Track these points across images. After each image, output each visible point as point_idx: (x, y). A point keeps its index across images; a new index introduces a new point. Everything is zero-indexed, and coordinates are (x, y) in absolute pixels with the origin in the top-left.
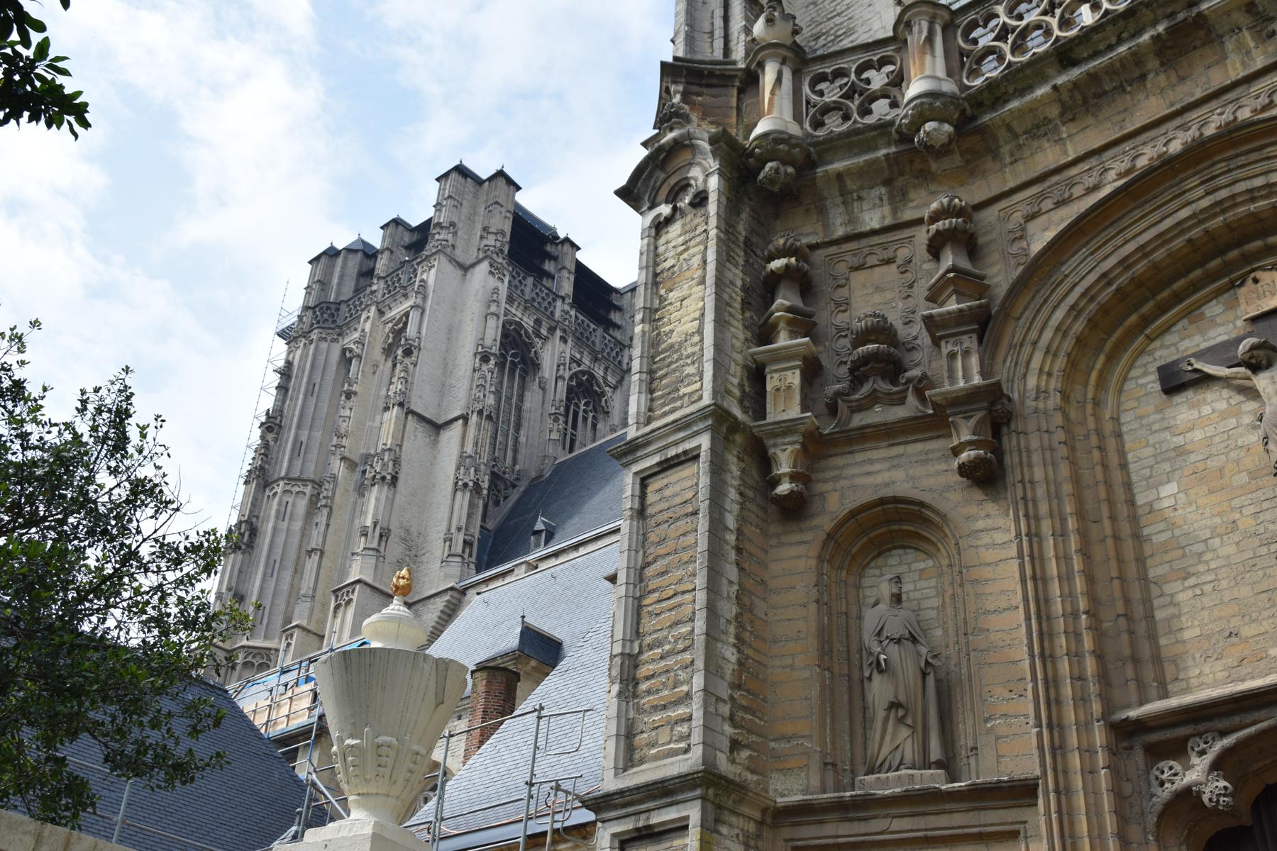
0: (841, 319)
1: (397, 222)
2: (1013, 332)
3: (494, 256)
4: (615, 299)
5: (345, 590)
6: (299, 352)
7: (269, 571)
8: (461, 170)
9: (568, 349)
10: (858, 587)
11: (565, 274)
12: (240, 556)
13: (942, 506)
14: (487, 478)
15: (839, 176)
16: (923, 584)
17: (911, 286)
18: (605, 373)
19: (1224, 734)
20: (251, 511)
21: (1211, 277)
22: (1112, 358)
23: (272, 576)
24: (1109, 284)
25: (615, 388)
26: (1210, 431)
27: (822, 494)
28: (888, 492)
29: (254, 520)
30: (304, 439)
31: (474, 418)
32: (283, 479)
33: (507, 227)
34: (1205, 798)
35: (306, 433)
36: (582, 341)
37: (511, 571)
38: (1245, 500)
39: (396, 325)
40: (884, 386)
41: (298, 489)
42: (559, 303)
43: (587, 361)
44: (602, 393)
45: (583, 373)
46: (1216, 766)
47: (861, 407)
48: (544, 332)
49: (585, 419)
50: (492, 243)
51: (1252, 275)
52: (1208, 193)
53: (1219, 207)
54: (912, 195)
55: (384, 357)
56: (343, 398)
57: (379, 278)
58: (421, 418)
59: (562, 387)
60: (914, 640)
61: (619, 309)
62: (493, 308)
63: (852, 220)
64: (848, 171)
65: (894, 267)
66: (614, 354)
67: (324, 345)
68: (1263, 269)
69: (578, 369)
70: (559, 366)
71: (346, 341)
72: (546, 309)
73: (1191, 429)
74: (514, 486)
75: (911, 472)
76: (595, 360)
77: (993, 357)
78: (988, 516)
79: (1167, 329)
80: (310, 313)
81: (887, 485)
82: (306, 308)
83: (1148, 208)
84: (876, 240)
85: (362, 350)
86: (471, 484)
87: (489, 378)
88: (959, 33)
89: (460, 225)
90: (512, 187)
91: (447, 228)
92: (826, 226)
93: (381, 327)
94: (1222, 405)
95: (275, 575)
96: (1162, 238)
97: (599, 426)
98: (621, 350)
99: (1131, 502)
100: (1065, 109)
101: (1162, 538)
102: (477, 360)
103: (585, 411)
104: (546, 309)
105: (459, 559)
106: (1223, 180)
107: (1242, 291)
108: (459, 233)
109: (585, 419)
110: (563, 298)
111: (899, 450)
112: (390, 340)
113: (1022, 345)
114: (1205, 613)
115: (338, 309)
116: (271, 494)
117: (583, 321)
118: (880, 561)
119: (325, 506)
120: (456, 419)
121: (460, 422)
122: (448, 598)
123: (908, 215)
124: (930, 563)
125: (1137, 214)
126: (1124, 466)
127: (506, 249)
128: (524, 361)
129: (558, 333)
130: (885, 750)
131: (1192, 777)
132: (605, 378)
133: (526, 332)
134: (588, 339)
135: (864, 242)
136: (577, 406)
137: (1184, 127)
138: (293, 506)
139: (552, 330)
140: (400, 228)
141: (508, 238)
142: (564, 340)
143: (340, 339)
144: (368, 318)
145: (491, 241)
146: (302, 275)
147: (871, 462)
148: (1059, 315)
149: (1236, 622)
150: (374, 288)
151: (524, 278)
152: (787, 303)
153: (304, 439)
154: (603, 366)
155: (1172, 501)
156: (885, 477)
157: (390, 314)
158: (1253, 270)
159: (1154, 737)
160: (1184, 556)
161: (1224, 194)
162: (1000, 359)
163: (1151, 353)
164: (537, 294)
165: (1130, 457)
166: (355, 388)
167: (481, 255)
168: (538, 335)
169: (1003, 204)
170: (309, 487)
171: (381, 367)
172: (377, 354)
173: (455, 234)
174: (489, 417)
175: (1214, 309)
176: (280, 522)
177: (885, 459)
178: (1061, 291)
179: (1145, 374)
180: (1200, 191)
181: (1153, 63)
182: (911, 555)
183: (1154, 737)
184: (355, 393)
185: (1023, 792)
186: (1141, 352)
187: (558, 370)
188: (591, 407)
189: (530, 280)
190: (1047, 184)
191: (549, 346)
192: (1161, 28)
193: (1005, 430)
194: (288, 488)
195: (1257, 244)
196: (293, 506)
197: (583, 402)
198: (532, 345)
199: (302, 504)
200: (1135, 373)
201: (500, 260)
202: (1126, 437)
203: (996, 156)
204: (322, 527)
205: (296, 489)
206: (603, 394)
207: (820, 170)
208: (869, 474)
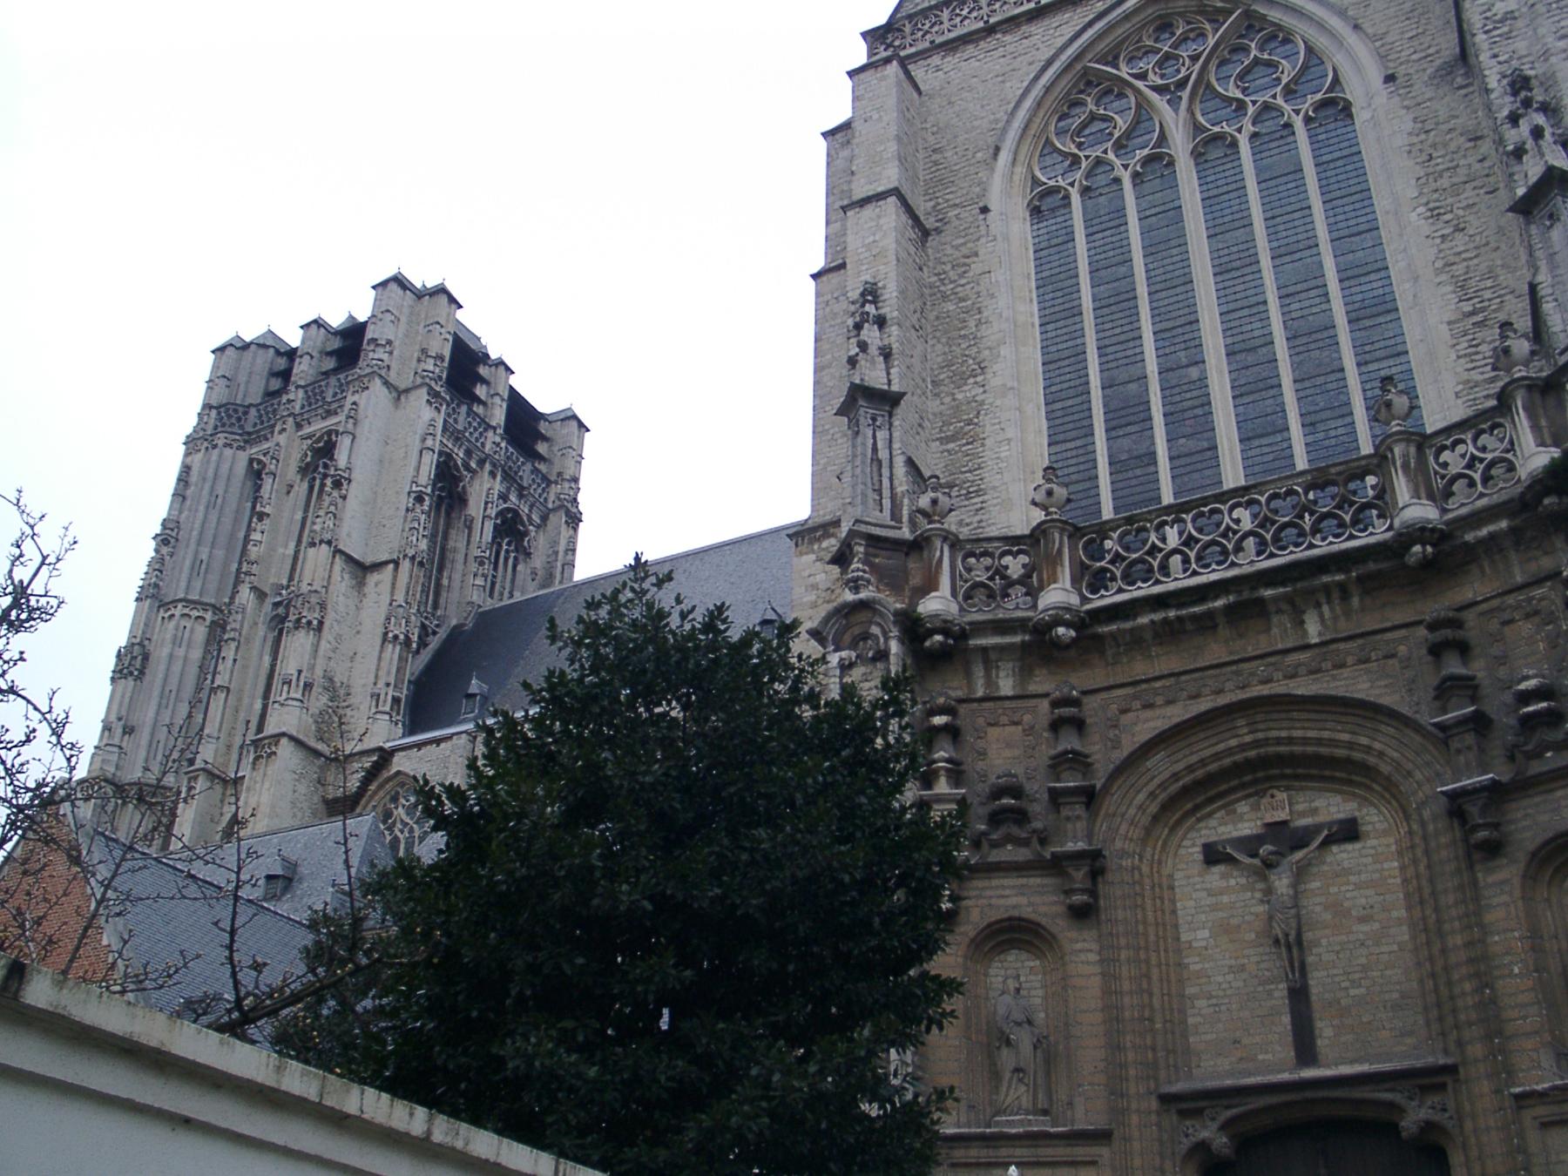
0: (980, 765)
1: (318, 323)
2: (1109, 804)
3: (433, 384)
4: (543, 427)
7: (164, 701)
8: (399, 281)
10: (986, 975)
11: (497, 400)
12: (131, 682)
13: (1054, 929)
14: (416, 631)
15: (984, 650)
16: (1032, 978)
17: (1034, 749)
19: (1228, 1107)
20: (144, 633)
21: (1243, 786)
22: (1173, 829)
23: (167, 707)
24: (1177, 780)
25: (538, 527)
26: (1233, 898)
27: (967, 908)
28: (1016, 913)
29: (146, 642)
30: (204, 557)
31: (406, 565)
33: (447, 353)
34: (1213, 1147)
35: (207, 550)
36: (510, 477)
37: (450, 737)
38: (1251, 951)
39: (315, 442)
40: (1015, 831)
41: (197, 614)
43: (513, 498)
45: (508, 510)
46: (1223, 1128)
47: (995, 845)
48: (473, 465)
49: (506, 559)
50: (431, 368)
51: (1270, 792)
52: (1251, 732)
53: (1256, 744)
54: (1037, 672)
55: (299, 477)
56: (255, 520)
57: (298, 387)
58: (350, 559)
59: (489, 527)
60: (1029, 1022)
61: (545, 439)
62: (429, 443)
63: (990, 682)
64: (996, 648)
65: (1020, 728)
66: (539, 491)
67: (228, 452)
68: (1278, 788)
70: (486, 503)
71: (253, 451)
72: (477, 440)
73: (1221, 894)
74: (435, 633)
75: (1032, 899)
76: (521, 496)
77: (1095, 821)
78: (1084, 940)
79: (1210, 815)
80: (214, 413)
81: (1014, 907)
82: (207, 406)
83: (1210, 732)
84: (1007, 704)
86: (402, 637)
87: (422, 522)
88: (1080, 546)
89: (396, 343)
90: (454, 306)
91: (384, 346)
92: (970, 685)
93: (298, 441)
94: (1243, 881)
95: (171, 707)
96: (1217, 757)
97: (519, 568)
98: (548, 486)
99: (1178, 939)
100: (1156, 635)
101: (1198, 967)
102: (411, 500)
103: (507, 551)
104: (477, 440)
105: (387, 717)
106: (1261, 726)
107: (1265, 801)
108: (395, 353)
109: (506, 559)
111: (1024, 881)
112: (309, 459)
113: (1114, 815)
114: (1220, 1025)
115: (246, 413)
116: (166, 615)
118: (1002, 956)
119: (233, 639)
120: (386, 563)
121: (391, 566)
122: (375, 758)
123: (1033, 688)
124: (1038, 963)
125: (1202, 735)
126: (1174, 912)
127: (444, 376)
128: (450, 496)
130: (1009, 1100)
131: (1204, 1134)
133: (456, 464)
134: (516, 473)
135: (999, 703)
136: (500, 545)
137: (1238, 673)
138: (192, 631)
139: (481, 463)
140: (322, 330)
141: (446, 364)
142: (493, 474)
145: (430, 365)
146: (203, 366)
147: (1003, 887)
148: (1141, 797)
149: (1238, 1034)
150: (292, 396)
151: (458, 405)
152: (946, 755)
153: (204, 557)
155: (1204, 944)
156: (1014, 901)
157: (307, 430)
158: (1271, 787)
159: (1184, 1106)
160: (1210, 983)
161: (1260, 735)
162: (1098, 824)
163: (1198, 830)
164: (470, 423)
165: (1178, 904)
166: (267, 510)
167: (419, 380)
169: (1104, 695)
170: (210, 613)
171: (296, 488)
172: (291, 473)
173: (391, 353)
174: (421, 564)
175: (1243, 808)
176: (177, 649)
177: (1013, 887)
178: (1144, 779)
179: (1194, 845)
180: (1245, 730)
181: (1221, 620)
182: (1024, 955)
183: (1184, 1106)
184: (268, 515)
185: (1101, 1136)
186: (1191, 828)
187: (485, 509)
188: (512, 548)
189: (464, 409)
190: (1138, 689)
191: (476, 483)
192: (1231, 598)
193: (1100, 879)
194: (186, 611)
195: (1276, 772)
196: (192, 631)
197: (506, 540)
198: (459, 479)
199: (201, 632)
200: (1185, 843)
201: (438, 389)
202: (1177, 890)
203: (1102, 653)
204: (230, 662)
205: (195, 613)
206: (526, 533)
207: (972, 642)
208: (1003, 897)
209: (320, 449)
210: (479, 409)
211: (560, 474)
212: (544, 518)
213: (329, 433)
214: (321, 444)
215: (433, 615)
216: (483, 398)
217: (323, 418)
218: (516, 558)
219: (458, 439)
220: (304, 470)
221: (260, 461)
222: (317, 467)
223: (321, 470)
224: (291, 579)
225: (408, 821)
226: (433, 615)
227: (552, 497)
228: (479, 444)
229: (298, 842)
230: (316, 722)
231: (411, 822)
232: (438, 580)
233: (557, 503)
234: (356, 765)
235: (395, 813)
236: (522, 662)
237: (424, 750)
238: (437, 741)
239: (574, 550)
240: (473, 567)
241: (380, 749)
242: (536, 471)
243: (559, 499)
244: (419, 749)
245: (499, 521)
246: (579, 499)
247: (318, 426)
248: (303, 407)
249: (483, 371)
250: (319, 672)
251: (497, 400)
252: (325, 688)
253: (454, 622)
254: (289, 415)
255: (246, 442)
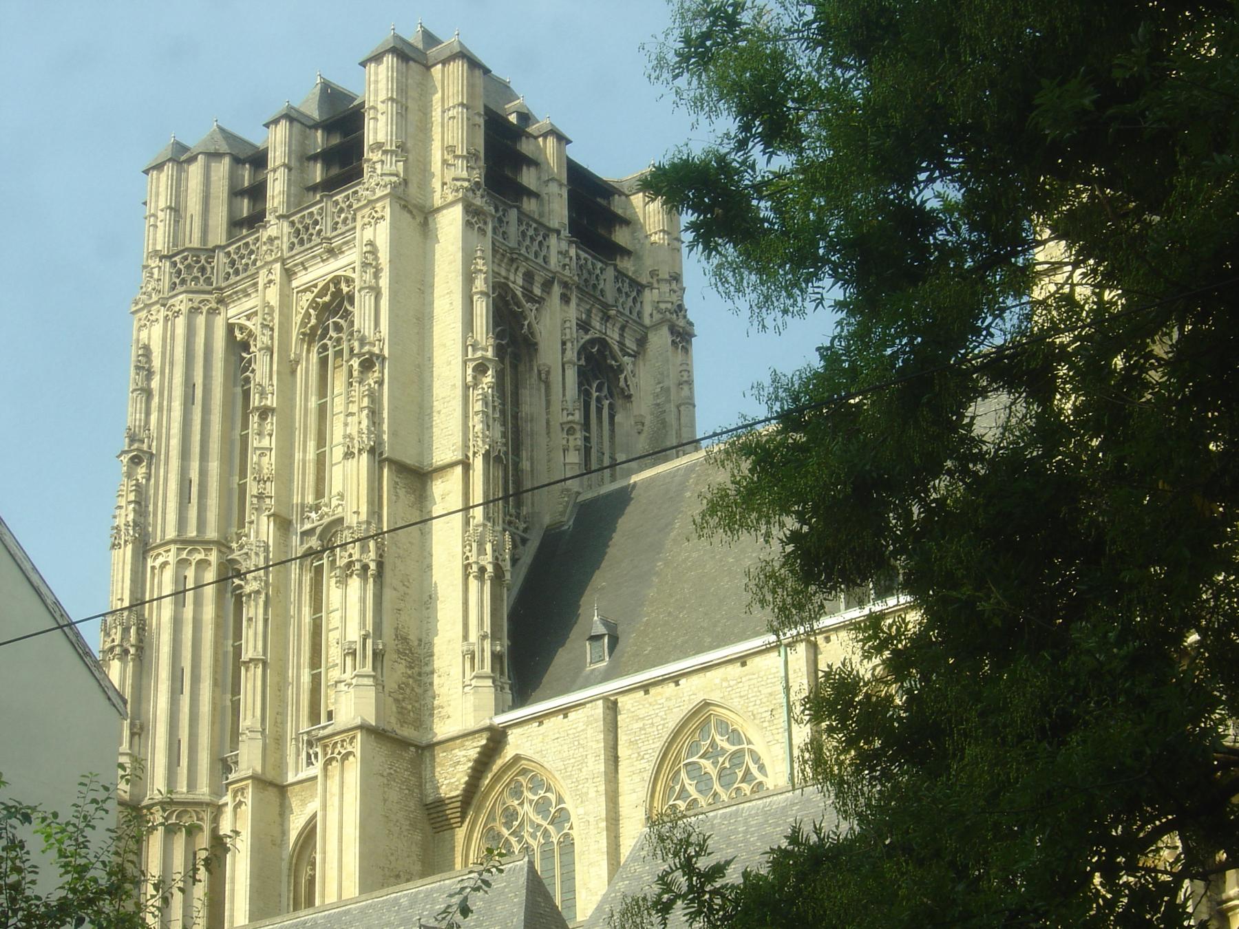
4: (617, 206)
5: (337, 738)
6: (157, 330)
9: (573, 312)
18: (622, 335)
25: (635, 356)
32: (173, 542)
36: (587, 290)
39: (320, 295)
42: (553, 240)
44: (619, 366)
45: (592, 342)
48: (537, 291)
49: (599, 410)
59: (572, 375)
61: (626, 222)
69: (588, 337)
70: (564, 343)
76: (606, 318)
85: (272, 338)
97: (618, 418)
98: (639, 292)
102: (469, 371)
103: (599, 400)
110: (558, 232)
112: (313, 321)
117: (586, 259)
120: (452, 465)
129: (557, 290)
132: (621, 344)
134: (595, 286)
139: (547, 285)
140: (297, 126)
142: (565, 299)
143: (222, 309)
144: (270, 282)
154: (618, 325)
168: (531, 297)
174: (498, 459)
184: (273, 410)
187: (564, 351)
188: (605, 392)
189: (513, 214)
198: (522, 316)
206: (620, 369)
209: (326, 306)
210: (530, 205)
211: (653, 273)
212: (642, 342)
213: (336, 281)
214: (327, 299)
215: (518, 517)
216: (533, 187)
217: (323, 261)
218: (611, 406)
219: (512, 260)
220: (310, 337)
221: (242, 328)
222: (326, 330)
223: (332, 333)
224: (319, 493)
225: (538, 820)
226: (518, 517)
227: (648, 309)
228: (540, 261)
229: (434, 902)
230: (397, 700)
231: (545, 824)
232: (516, 465)
233: (657, 317)
234: (459, 753)
235: (521, 811)
236: (655, 579)
237: (550, 723)
238: (564, 711)
239: (690, 383)
240: (560, 438)
241: (490, 729)
242: (620, 275)
243: (660, 311)
244: (541, 723)
245: (583, 362)
246: (687, 305)
247: (319, 272)
248: (291, 248)
249: (526, 147)
250: (388, 631)
251: (553, 188)
252: (398, 652)
253: (547, 520)
254: (275, 261)
255: (220, 301)
